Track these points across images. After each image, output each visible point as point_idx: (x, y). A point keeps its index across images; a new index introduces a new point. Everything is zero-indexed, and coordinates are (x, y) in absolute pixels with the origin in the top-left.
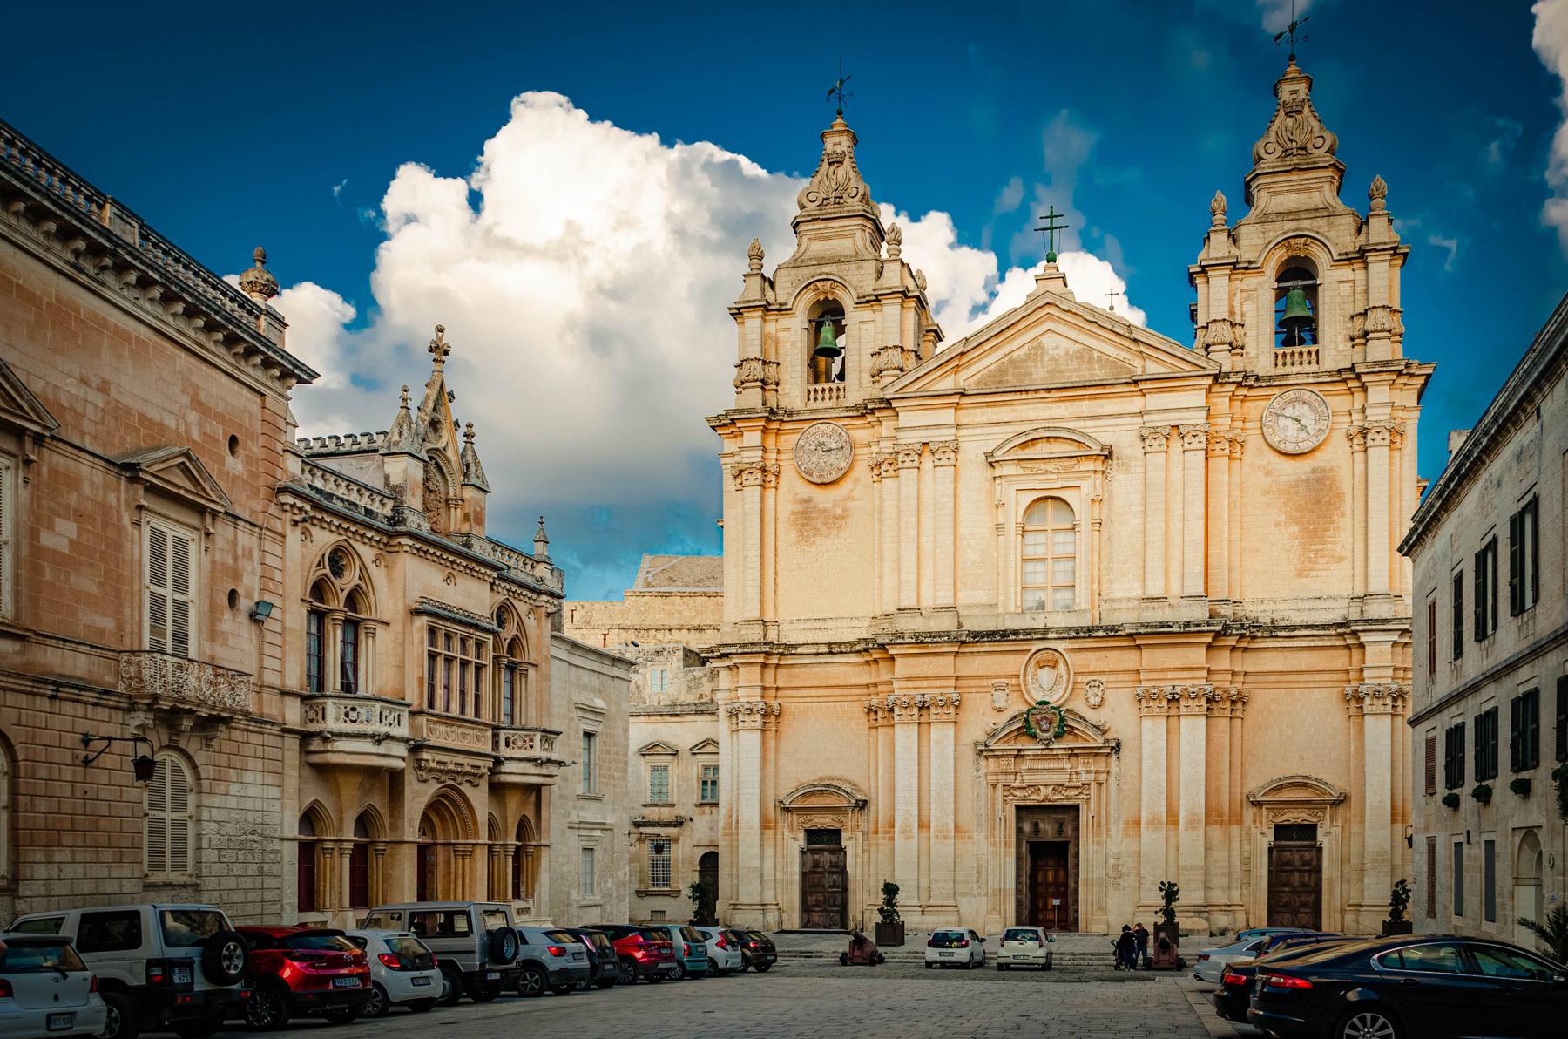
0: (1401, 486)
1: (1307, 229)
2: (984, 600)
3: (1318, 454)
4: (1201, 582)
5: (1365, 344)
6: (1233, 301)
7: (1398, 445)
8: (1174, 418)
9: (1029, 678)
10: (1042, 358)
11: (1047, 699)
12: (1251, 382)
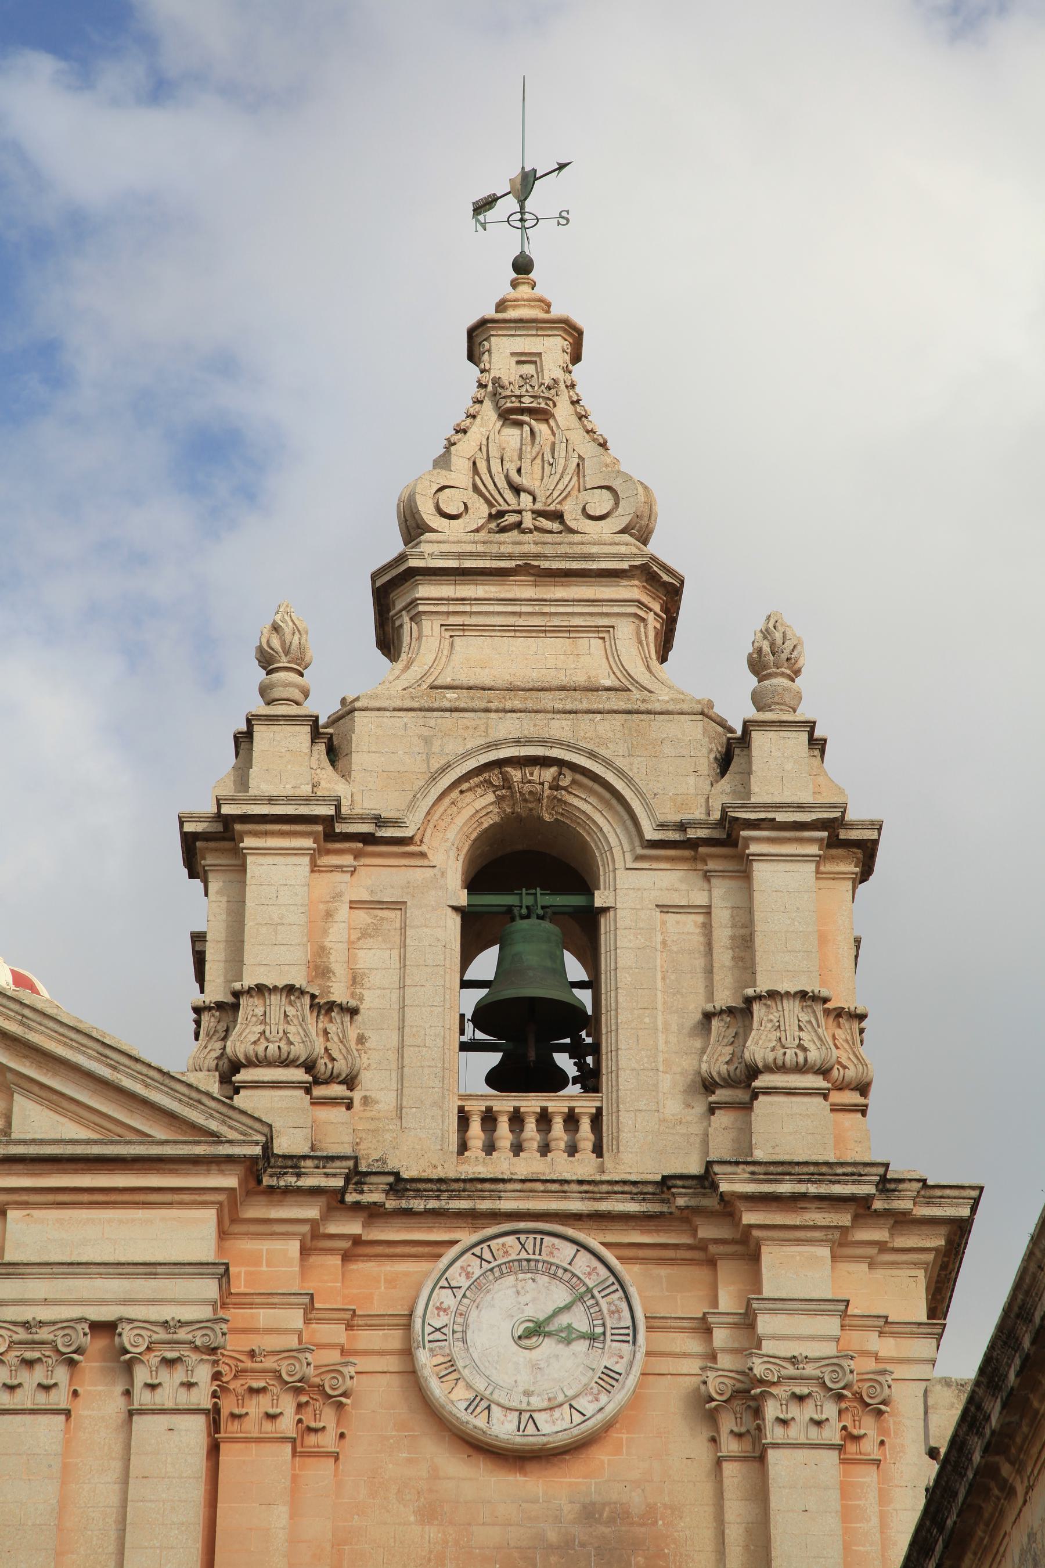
1: (561, 744)
5: (747, 1107)
6: (325, 932)
7: (869, 1447)
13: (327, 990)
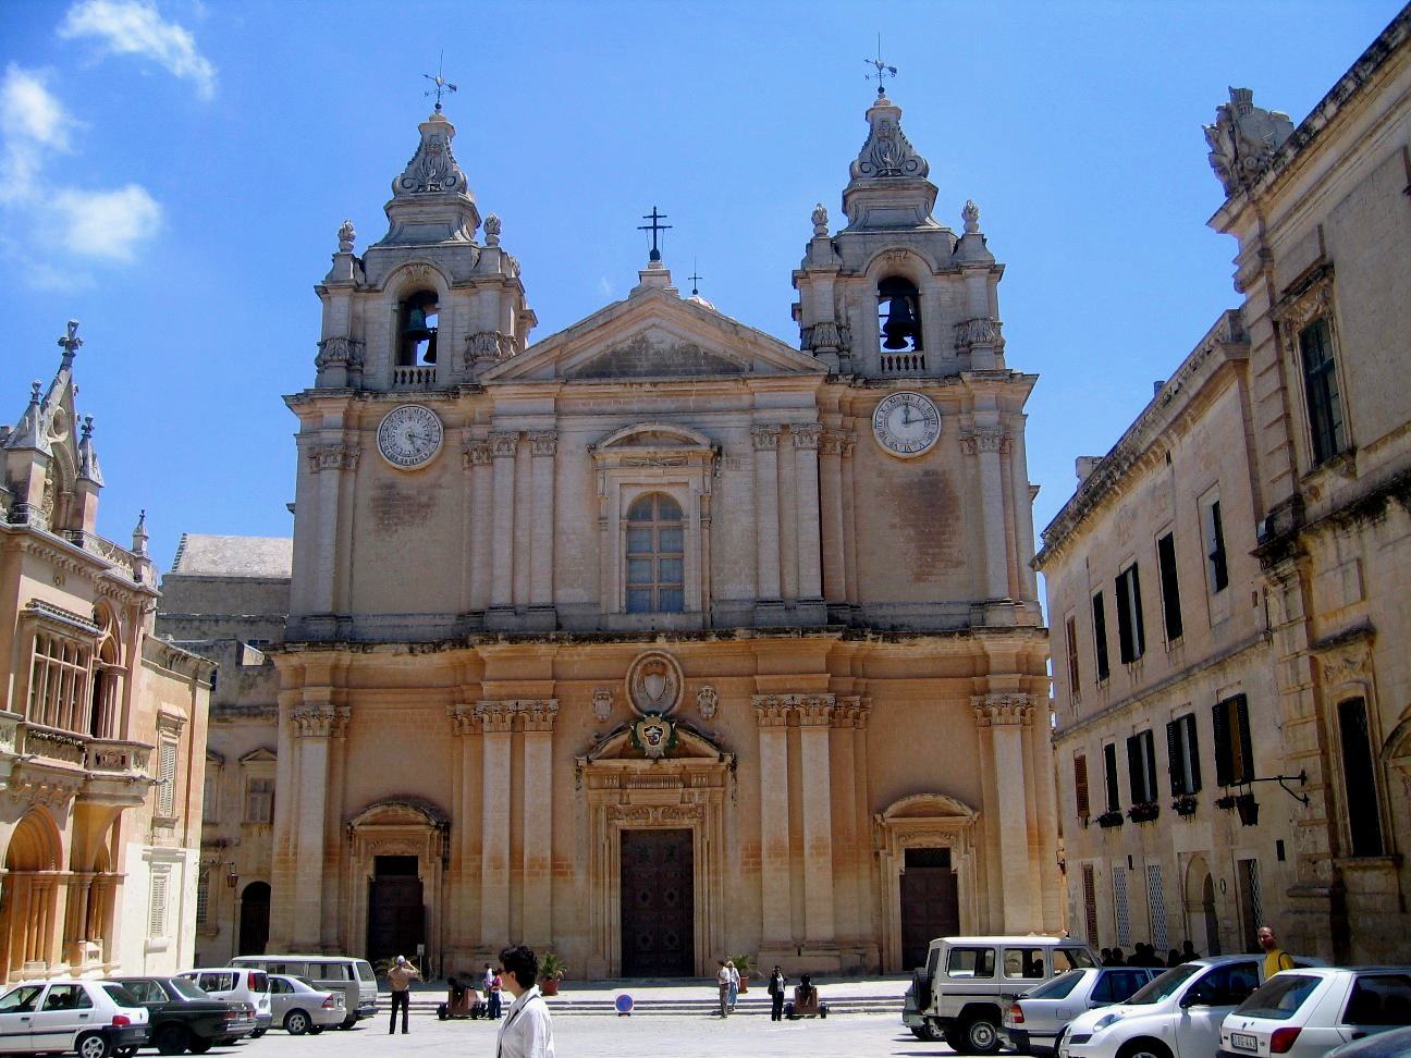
0: (1013, 491)
2: (585, 599)
3: (930, 458)
4: (818, 585)
8: (784, 416)
9: (635, 685)
10: (647, 351)
11: (656, 709)
12: (860, 382)
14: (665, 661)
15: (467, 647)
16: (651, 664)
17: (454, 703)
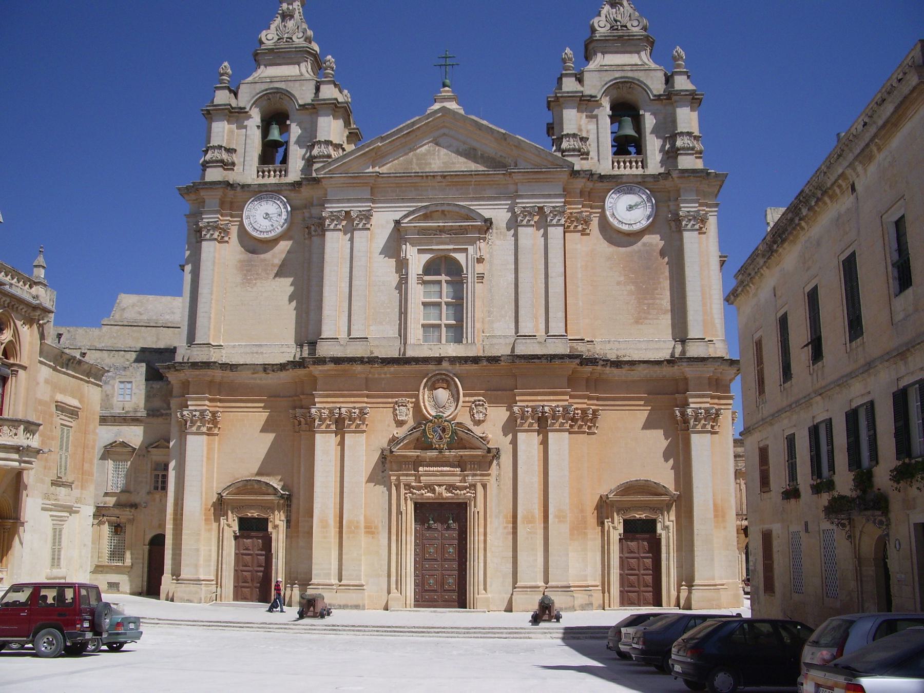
5: (676, 158)
6: (580, 121)
10: (438, 155)
13: (582, 134)
14: (449, 379)
15: (305, 367)
16: (438, 380)
17: (294, 408)
